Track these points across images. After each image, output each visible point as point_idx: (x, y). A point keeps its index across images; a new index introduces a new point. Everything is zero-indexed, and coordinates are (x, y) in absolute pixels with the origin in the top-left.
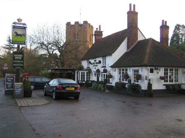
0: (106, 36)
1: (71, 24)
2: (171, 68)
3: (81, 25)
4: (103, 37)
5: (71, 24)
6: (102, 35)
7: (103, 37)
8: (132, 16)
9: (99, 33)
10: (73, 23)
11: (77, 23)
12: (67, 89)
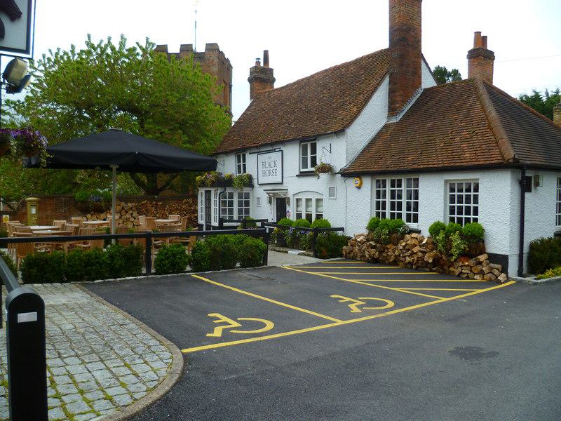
0: (284, 84)
1: (170, 51)
2: (396, 178)
3: (200, 56)
4: (277, 85)
5: (170, 51)
6: (274, 80)
7: (277, 85)
8: (109, 39)
9: (261, 76)
10: (174, 49)
11: (186, 48)
12: (34, 232)
